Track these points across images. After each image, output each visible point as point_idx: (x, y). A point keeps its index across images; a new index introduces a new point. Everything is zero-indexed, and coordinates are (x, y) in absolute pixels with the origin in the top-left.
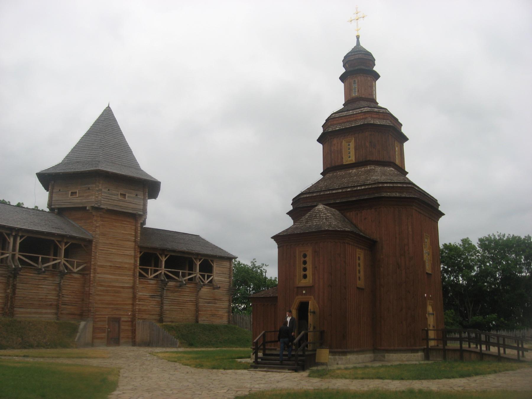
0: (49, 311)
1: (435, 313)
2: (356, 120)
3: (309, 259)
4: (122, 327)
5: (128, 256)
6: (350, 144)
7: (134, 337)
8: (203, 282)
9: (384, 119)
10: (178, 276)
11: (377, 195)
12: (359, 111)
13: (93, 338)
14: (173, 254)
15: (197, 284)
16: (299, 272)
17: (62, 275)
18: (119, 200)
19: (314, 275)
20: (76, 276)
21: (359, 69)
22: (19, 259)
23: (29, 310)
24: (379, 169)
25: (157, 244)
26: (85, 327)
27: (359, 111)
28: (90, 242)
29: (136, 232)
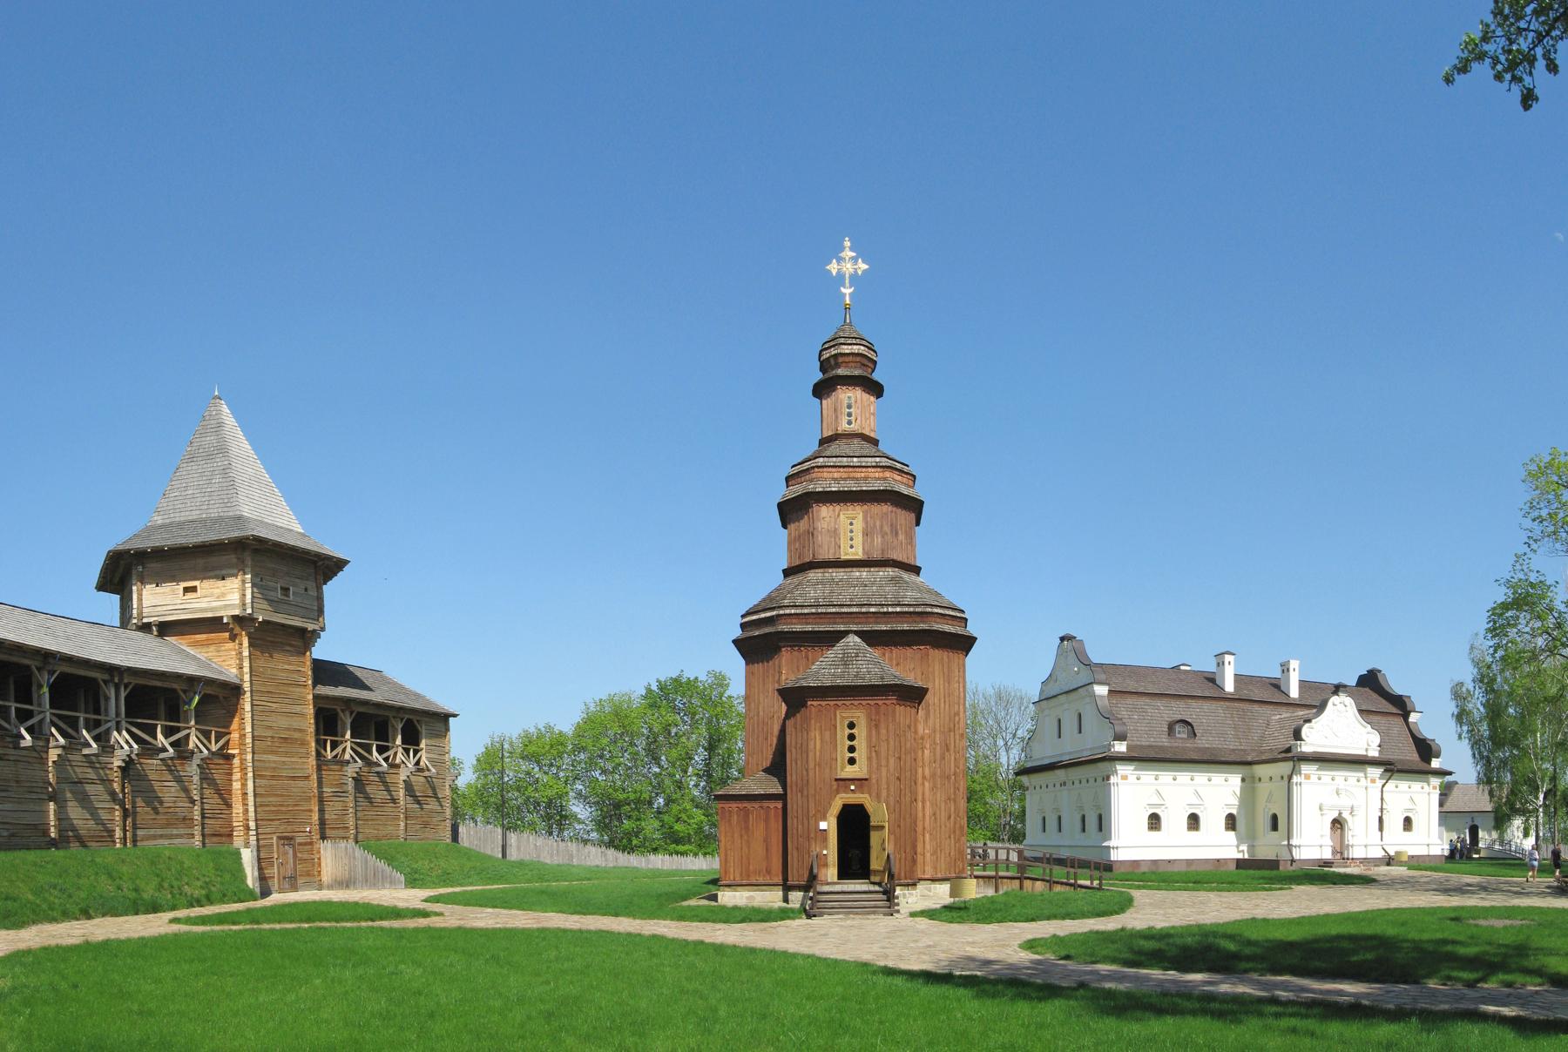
19: (869, 759)
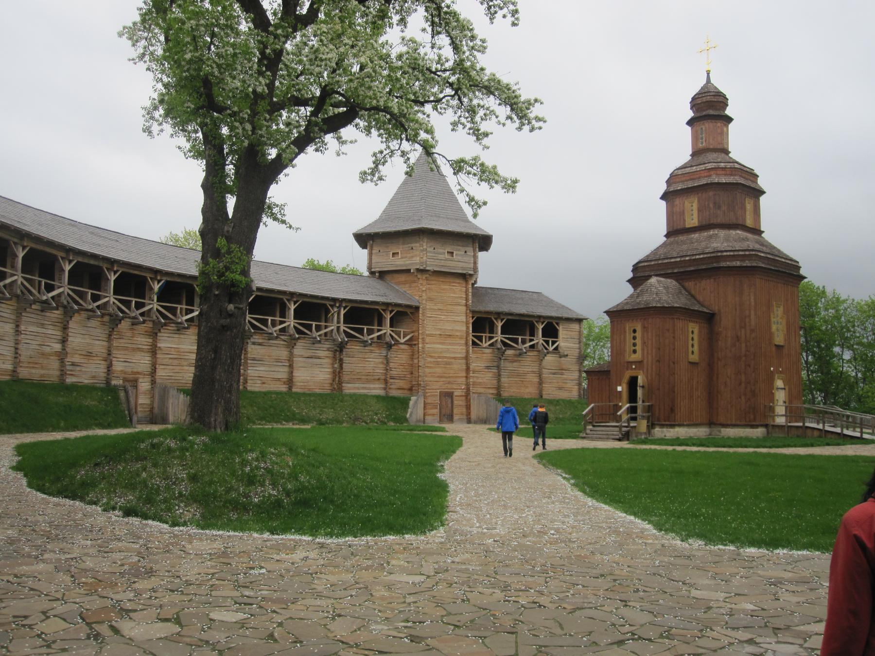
0: (377, 386)
1: (787, 388)
2: (699, 178)
3: (638, 335)
4: (455, 402)
5: (459, 323)
7: (468, 414)
8: (546, 349)
9: (731, 175)
10: (517, 344)
12: (702, 167)
13: (424, 415)
14: (510, 317)
15: (539, 351)
17: (389, 346)
18: (446, 260)
19: (643, 350)
20: (403, 347)
21: (710, 109)
22: (345, 331)
23: (357, 385)
24: (722, 233)
25: (492, 307)
26: (416, 402)
27: (702, 167)
28: (417, 308)
29: (467, 295)
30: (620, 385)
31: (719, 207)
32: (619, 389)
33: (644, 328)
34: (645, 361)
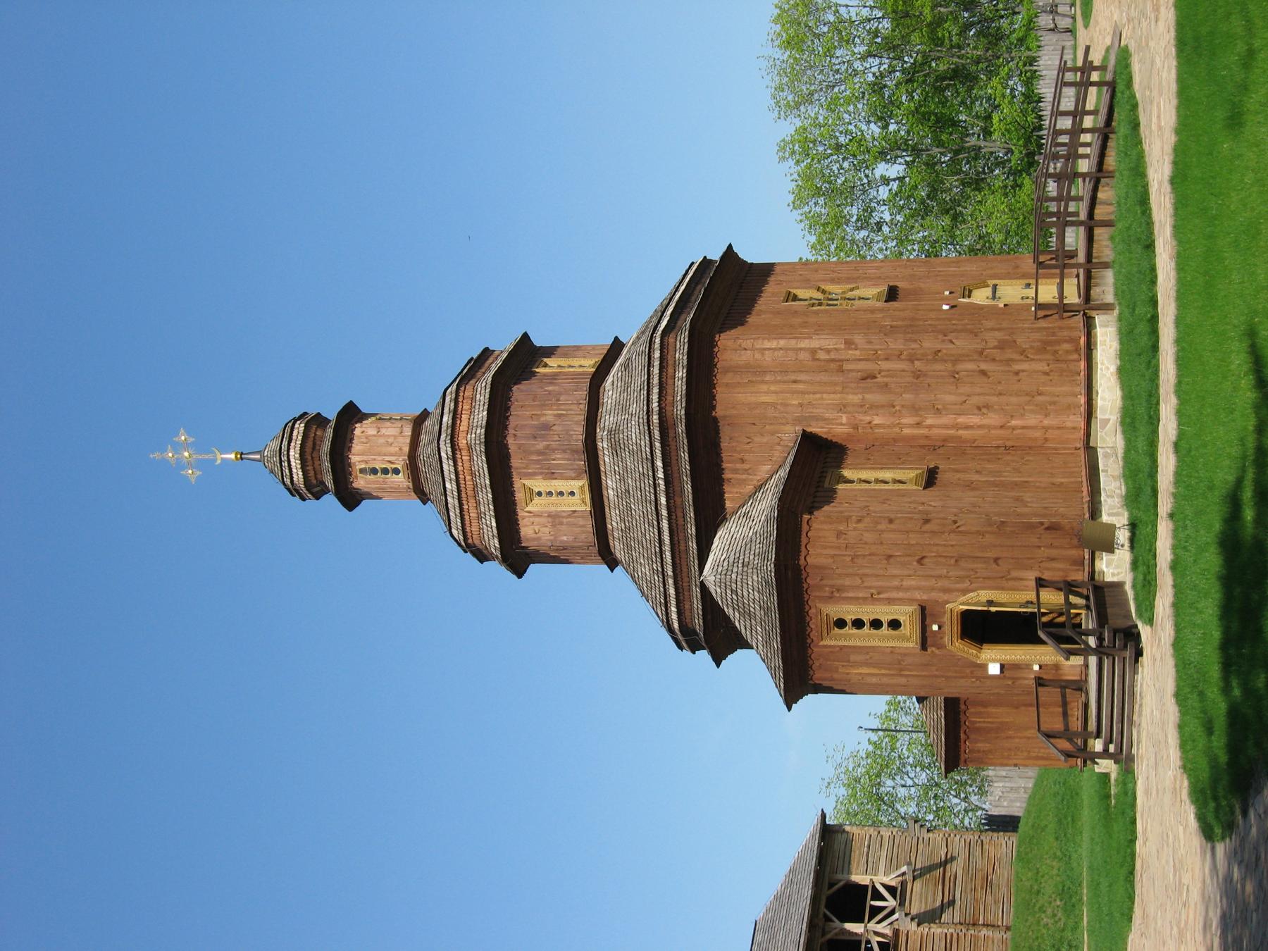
3: (850, 612)
6: (536, 490)
11: (681, 428)
12: (447, 466)
16: (882, 639)
19: (890, 601)
30: (984, 667)
31: (547, 427)
32: (994, 669)
33: (830, 598)
34: (918, 595)
